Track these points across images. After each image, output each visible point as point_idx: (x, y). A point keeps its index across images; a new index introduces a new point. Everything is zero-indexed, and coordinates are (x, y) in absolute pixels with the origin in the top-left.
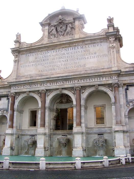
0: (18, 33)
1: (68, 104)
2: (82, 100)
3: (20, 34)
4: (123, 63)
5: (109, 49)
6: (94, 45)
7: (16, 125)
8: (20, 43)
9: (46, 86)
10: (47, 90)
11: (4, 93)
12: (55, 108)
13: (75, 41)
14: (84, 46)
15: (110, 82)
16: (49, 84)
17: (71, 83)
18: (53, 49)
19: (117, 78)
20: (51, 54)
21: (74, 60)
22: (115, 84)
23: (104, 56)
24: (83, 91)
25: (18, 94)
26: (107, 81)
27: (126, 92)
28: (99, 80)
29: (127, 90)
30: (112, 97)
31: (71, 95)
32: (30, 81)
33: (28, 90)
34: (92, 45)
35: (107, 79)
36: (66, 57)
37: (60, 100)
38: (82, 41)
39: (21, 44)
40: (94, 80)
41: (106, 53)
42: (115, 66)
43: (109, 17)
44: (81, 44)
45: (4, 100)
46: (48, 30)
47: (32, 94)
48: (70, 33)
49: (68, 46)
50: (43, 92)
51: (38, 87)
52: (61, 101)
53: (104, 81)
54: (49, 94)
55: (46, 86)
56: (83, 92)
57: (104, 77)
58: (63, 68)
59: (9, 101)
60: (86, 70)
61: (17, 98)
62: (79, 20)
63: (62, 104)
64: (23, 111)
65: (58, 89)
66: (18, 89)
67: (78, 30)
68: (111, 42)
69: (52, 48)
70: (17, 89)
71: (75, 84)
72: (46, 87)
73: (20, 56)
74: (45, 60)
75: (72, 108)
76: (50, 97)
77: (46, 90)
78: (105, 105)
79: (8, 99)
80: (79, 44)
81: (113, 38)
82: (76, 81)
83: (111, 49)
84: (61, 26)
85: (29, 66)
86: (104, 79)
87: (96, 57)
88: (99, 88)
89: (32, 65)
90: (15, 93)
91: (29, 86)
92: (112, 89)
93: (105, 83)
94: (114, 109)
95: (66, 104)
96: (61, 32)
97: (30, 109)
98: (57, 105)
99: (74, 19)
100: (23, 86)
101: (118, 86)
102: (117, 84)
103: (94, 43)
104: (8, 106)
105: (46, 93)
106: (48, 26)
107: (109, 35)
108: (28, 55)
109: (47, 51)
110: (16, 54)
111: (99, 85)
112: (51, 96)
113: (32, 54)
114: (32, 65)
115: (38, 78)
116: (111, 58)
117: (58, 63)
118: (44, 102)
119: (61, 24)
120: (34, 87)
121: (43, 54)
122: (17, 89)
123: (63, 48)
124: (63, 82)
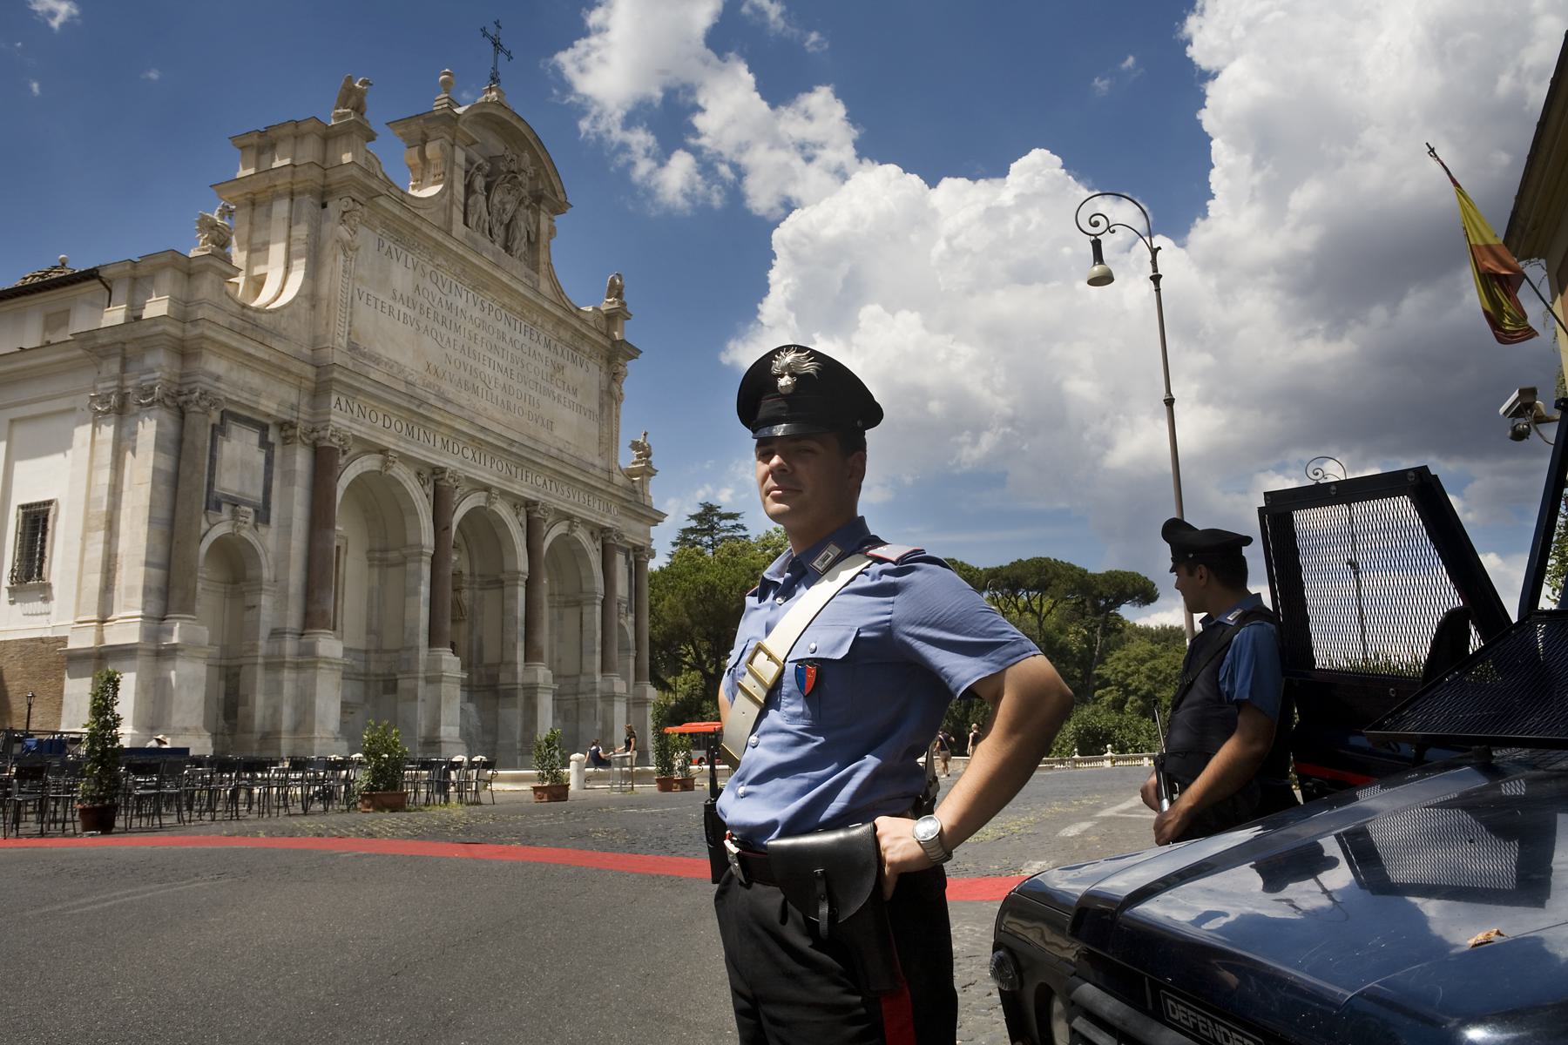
33: (403, 447)
38: (559, 319)
79: (264, 444)
100: (381, 416)
103: (577, 349)
115: (432, 401)
117: (489, 371)
123: (504, 306)
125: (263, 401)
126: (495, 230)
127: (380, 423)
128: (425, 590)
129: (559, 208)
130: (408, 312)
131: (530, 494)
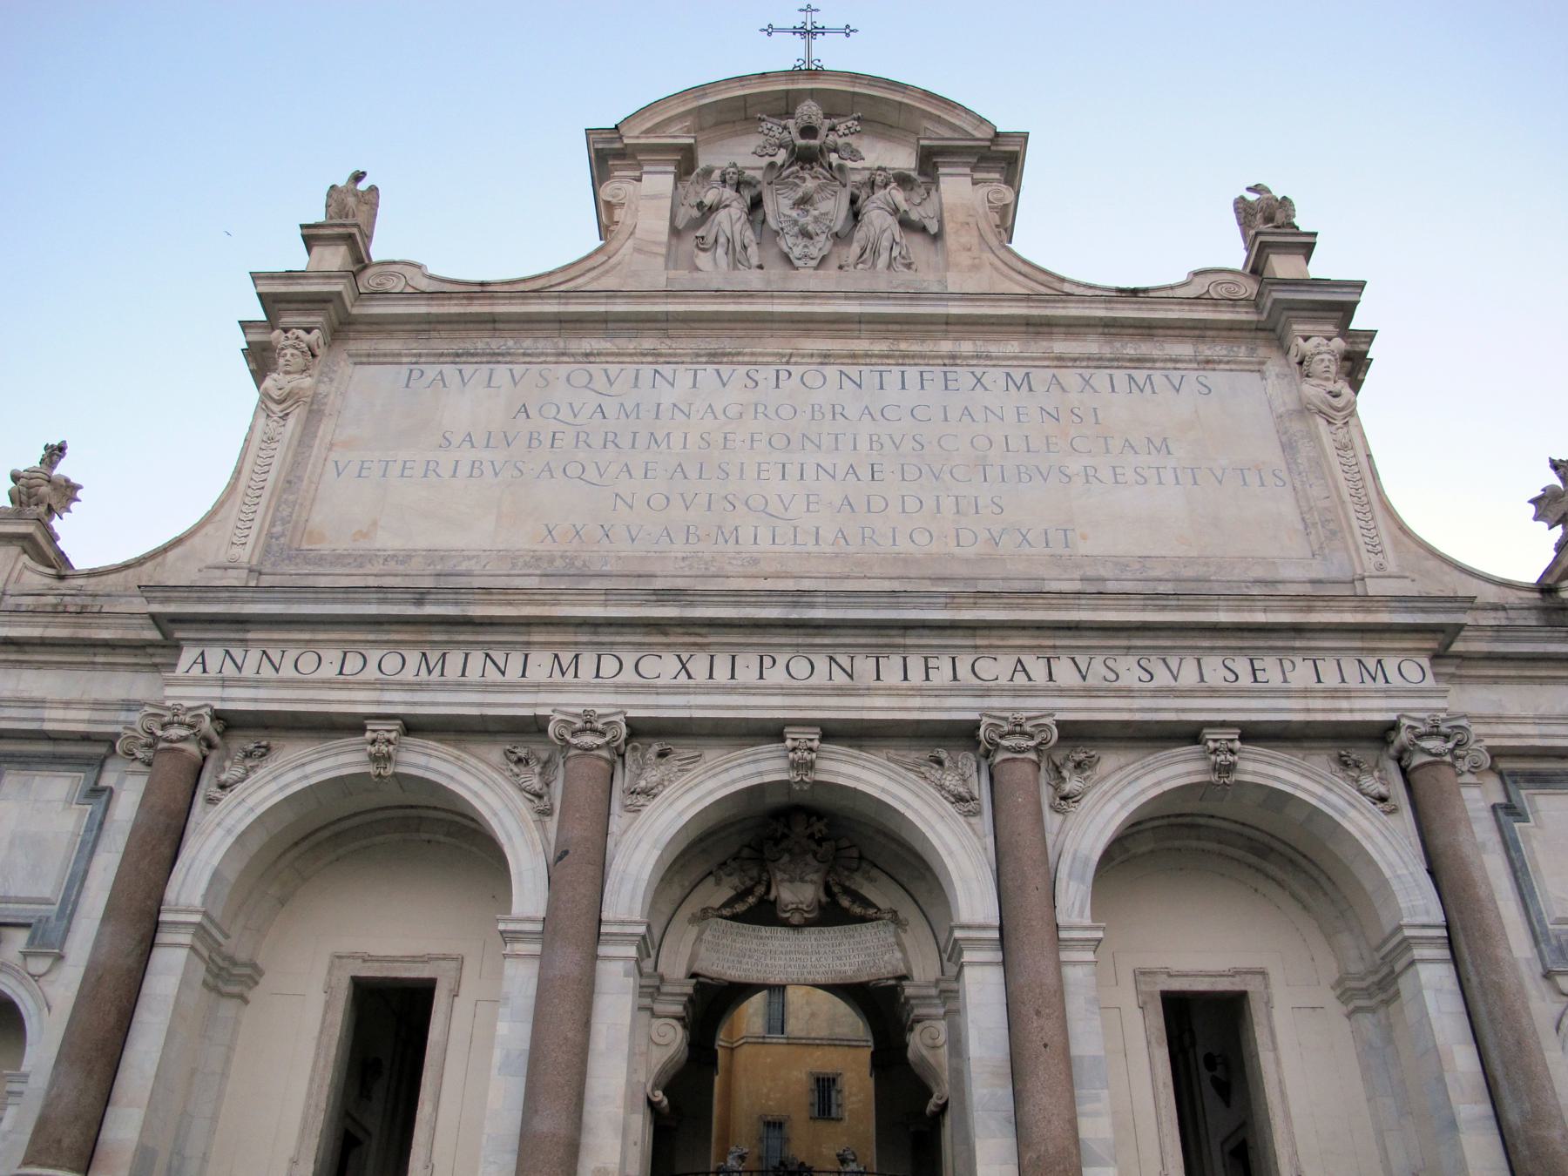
0: (358, 177)
1: (832, 934)
2: (1070, 875)
3: (373, 190)
4: (1432, 564)
5: (1296, 426)
6: (1140, 375)
7: (146, 1127)
8: (361, 262)
9: (629, 676)
10: (639, 730)
11: (55, 719)
12: (674, 967)
13: (955, 309)
14: (1040, 376)
15: (1374, 710)
16: (663, 667)
17: (942, 675)
18: (714, 357)
19: (1430, 682)
20: (692, 396)
21: (947, 477)
22: (1429, 735)
23: (1253, 478)
24: (1072, 784)
25: (249, 730)
26: (1333, 693)
27: (1510, 846)
28: (1246, 680)
29: (1516, 825)
30: (1402, 871)
31: (927, 813)
32: (437, 602)
33: (399, 702)
34: (1120, 375)
35: (1331, 680)
36: (863, 445)
37: (735, 880)
39: (370, 272)
40: (1189, 677)
41: (1272, 456)
42: (1381, 567)
43: (1249, 189)
44: (1013, 347)
45: (46, 805)
46: (668, 203)
47: (434, 763)
48: (891, 260)
49: (881, 347)
50: (588, 740)
51: (538, 687)
52: (751, 900)
53: (1306, 693)
54: (651, 776)
55: (629, 676)
56: (1064, 798)
57: (1298, 660)
58: (828, 534)
59: (97, 827)
60: (1090, 572)
61: (223, 787)
62: (978, 176)
63: (765, 931)
64: (253, 975)
65: (772, 732)
66: (258, 683)
67: (975, 241)
68: (1317, 368)
69: (713, 345)
70: (248, 672)
71: (985, 693)
72: (627, 688)
73: (345, 368)
74: (625, 442)
75: (951, 953)
76: (671, 813)
77: (630, 722)
78: (1263, 973)
80: (994, 349)
81: (1329, 339)
82: (987, 668)
83: (1321, 422)
84: (810, 184)
85: (430, 468)
86: (1301, 673)
87: (1168, 476)
88: (1250, 766)
89: (464, 469)
90: (217, 716)
91: (413, 657)
92: (1383, 790)
93: (1320, 711)
94: (1454, 1004)
95: (812, 939)
96: (806, 234)
97: (352, 956)
98: (699, 939)
99: (930, 160)
101: (1448, 758)
102: (1447, 737)
103: (1140, 361)
104: (78, 880)
105: (612, 764)
106: (671, 178)
107: (1292, 306)
108: (431, 371)
109: (647, 371)
110: (301, 333)
111: (1253, 734)
112: (680, 805)
113: (477, 373)
114: (464, 469)
116: (1327, 503)
118: (581, 864)
119: (817, 183)
120: (473, 674)
121: (600, 382)
122: (248, 672)
123: (826, 358)
124: (844, 660)
125: (47, 714)
126: (797, 252)
127: (329, 671)
128: (512, 1032)
129: (1001, 157)
130: (486, 455)
131: (959, 709)
